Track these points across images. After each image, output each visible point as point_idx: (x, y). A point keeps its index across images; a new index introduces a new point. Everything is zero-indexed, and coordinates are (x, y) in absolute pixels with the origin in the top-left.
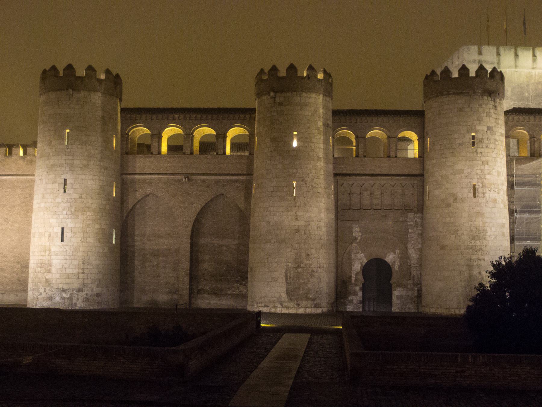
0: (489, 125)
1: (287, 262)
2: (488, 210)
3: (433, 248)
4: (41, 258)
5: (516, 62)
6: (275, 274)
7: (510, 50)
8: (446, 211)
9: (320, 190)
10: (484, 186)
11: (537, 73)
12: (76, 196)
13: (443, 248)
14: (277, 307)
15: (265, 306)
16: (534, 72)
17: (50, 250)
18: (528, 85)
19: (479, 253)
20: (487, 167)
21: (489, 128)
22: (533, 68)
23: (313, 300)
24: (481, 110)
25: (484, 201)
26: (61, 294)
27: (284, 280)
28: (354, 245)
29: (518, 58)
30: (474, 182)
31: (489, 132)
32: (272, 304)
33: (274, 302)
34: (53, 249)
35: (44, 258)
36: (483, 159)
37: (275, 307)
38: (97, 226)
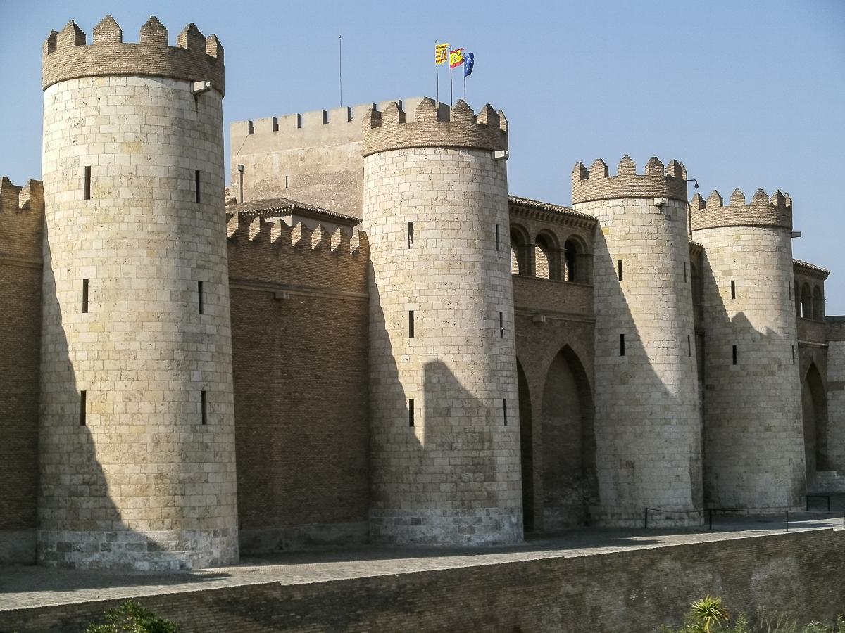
1: (691, 452)
3: (751, 430)
4: (475, 454)
6: (680, 471)
8: (770, 381)
13: (768, 429)
14: (683, 518)
15: (667, 518)
17: (491, 441)
26: (510, 517)
27: (689, 480)
32: (677, 514)
33: (679, 511)
34: (496, 438)
35: (482, 455)
37: (681, 519)
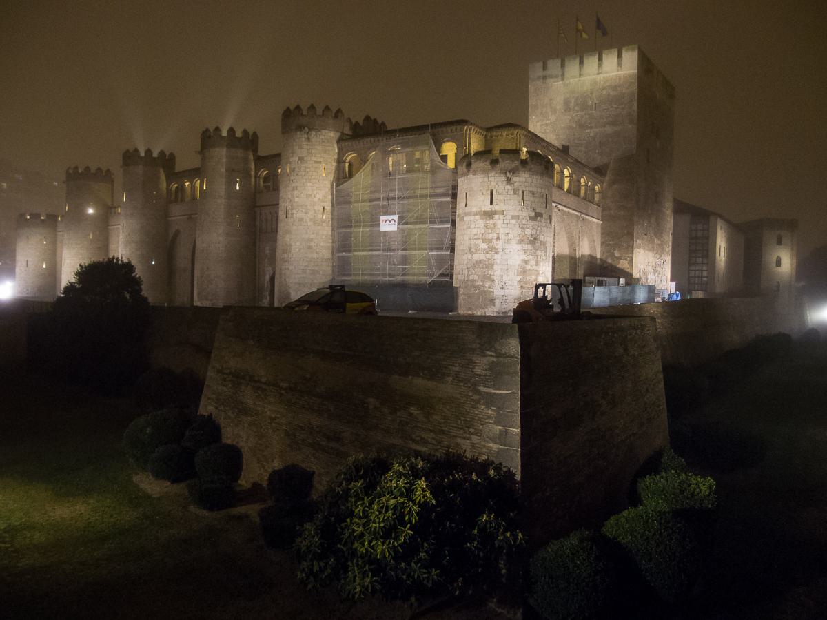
0: (300, 156)
2: (294, 227)
5: (580, 70)
7: (575, 59)
9: (219, 220)
10: (292, 209)
11: (602, 78)
12: (127, 234)
16: (599, 77)
18: (592, 93)
19: (286, 263)
20: (296, 192)
21: (301, 159)
22: (598, 74)
23: (211, 300)
24: (295, 144)
25: (292, 219)
28: (266, 260)
29: (583, 66)
30: (287, 205)
31: (299, 162)
36: (294, 185)
38: (138, 252)
